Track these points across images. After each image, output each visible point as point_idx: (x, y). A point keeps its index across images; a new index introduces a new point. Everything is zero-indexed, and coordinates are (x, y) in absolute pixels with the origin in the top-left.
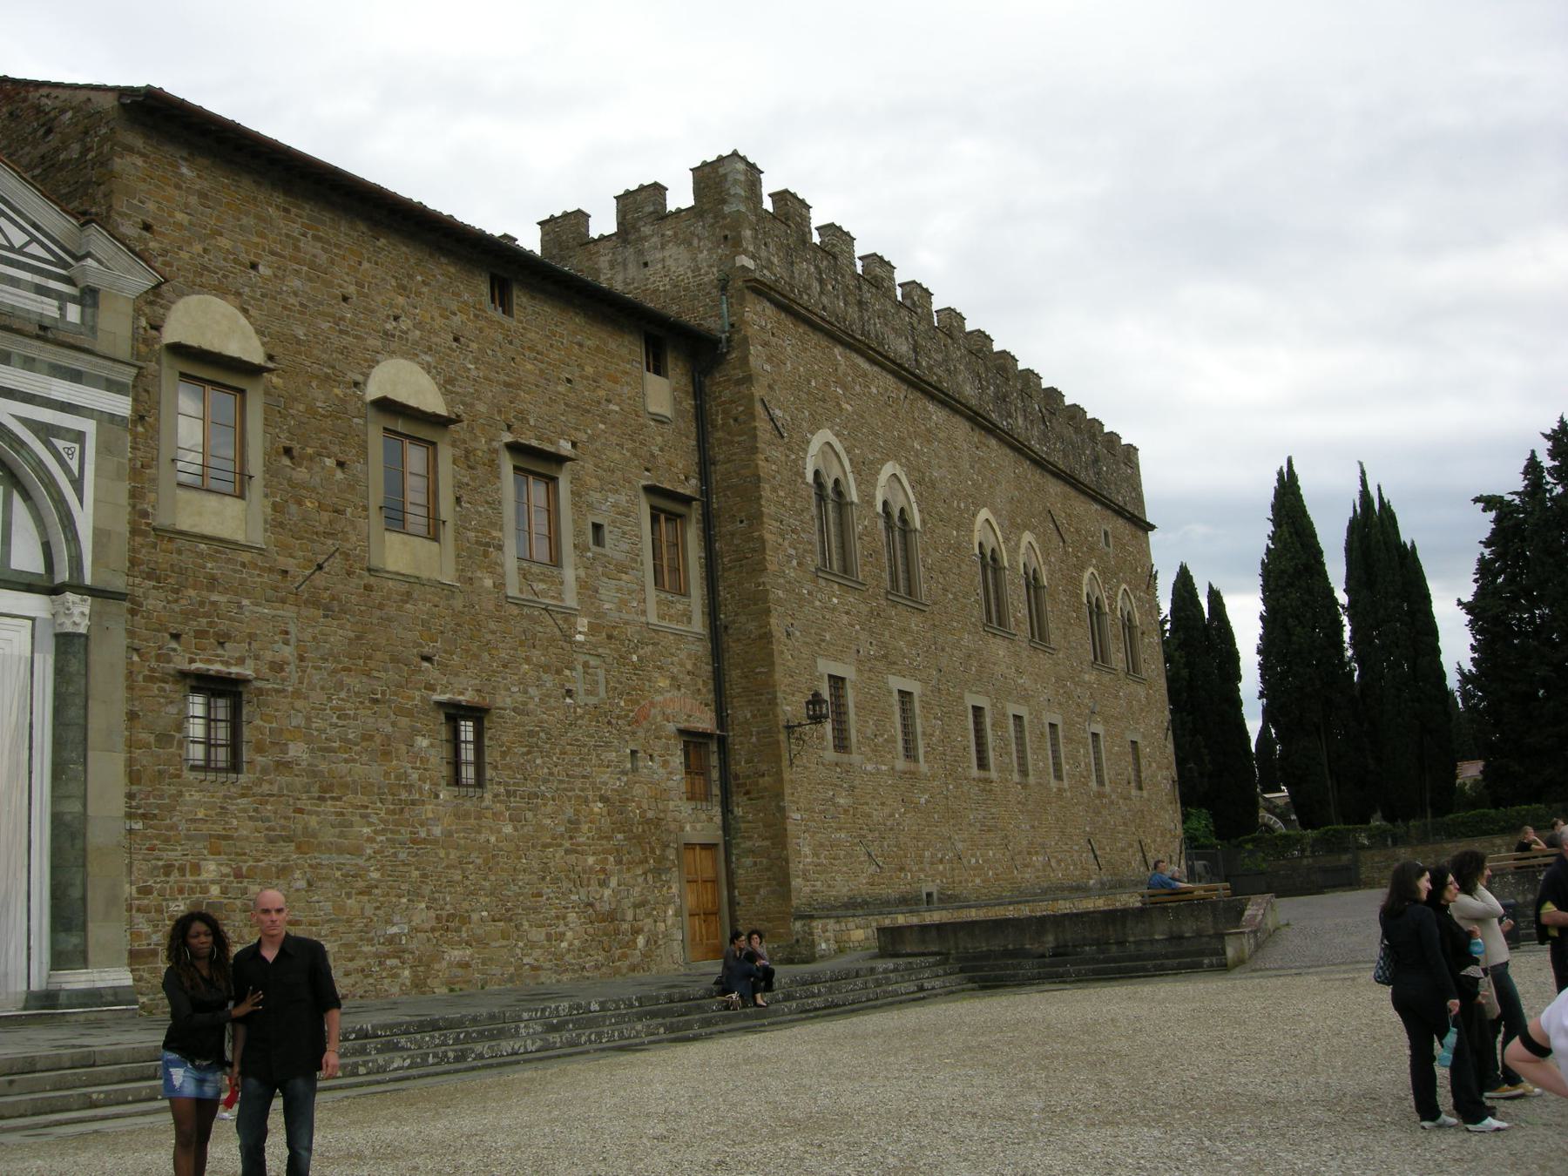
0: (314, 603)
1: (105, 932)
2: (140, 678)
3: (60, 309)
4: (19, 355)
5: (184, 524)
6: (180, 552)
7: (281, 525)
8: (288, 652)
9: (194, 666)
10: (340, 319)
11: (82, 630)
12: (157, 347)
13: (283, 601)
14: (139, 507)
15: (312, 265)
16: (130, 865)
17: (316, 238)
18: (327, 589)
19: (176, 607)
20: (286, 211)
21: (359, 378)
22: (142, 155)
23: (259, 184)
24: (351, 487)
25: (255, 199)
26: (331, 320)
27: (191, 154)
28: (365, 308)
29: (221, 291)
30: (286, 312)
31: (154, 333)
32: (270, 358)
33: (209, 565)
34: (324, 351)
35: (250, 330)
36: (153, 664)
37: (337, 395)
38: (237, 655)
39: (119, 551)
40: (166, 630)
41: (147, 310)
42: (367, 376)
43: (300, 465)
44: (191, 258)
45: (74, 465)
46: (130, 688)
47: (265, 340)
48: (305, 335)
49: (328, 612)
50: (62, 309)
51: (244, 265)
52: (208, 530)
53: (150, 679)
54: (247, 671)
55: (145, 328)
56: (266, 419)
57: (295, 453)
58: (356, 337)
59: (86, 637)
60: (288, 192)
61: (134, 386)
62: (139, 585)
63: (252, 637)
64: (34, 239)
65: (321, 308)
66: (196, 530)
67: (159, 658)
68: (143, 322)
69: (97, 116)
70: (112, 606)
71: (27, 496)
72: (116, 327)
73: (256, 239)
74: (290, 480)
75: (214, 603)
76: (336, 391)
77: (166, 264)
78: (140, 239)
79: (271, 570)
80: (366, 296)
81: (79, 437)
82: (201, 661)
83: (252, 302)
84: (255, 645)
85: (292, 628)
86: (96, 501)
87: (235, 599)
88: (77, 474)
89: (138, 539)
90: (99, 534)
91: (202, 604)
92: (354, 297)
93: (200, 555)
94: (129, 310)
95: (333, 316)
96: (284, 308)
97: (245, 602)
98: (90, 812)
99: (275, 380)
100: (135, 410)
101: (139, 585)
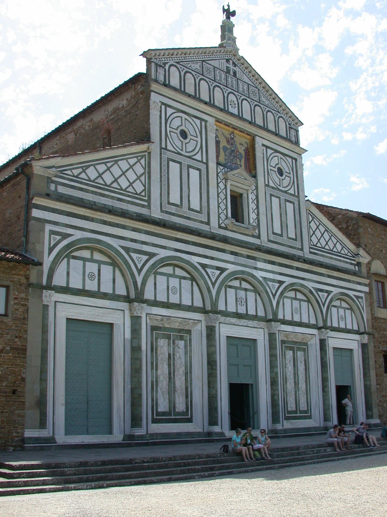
1: (375, 411)
9: (384, 349)
11: (367, 343)
16: (378, 396)
20: (385, 235)
22: (363, 228)
45: (362, 304)
46: (375, 355)
50: (355, 268)
53: (377, 353)
69: (351, 218)
71: (354, 313)
72: (364, 270)
81: (362, 298)
86: (366, 312)
89: (373, 321)
90: (367, 320)
98: (372, 384)
100: (369, 290)
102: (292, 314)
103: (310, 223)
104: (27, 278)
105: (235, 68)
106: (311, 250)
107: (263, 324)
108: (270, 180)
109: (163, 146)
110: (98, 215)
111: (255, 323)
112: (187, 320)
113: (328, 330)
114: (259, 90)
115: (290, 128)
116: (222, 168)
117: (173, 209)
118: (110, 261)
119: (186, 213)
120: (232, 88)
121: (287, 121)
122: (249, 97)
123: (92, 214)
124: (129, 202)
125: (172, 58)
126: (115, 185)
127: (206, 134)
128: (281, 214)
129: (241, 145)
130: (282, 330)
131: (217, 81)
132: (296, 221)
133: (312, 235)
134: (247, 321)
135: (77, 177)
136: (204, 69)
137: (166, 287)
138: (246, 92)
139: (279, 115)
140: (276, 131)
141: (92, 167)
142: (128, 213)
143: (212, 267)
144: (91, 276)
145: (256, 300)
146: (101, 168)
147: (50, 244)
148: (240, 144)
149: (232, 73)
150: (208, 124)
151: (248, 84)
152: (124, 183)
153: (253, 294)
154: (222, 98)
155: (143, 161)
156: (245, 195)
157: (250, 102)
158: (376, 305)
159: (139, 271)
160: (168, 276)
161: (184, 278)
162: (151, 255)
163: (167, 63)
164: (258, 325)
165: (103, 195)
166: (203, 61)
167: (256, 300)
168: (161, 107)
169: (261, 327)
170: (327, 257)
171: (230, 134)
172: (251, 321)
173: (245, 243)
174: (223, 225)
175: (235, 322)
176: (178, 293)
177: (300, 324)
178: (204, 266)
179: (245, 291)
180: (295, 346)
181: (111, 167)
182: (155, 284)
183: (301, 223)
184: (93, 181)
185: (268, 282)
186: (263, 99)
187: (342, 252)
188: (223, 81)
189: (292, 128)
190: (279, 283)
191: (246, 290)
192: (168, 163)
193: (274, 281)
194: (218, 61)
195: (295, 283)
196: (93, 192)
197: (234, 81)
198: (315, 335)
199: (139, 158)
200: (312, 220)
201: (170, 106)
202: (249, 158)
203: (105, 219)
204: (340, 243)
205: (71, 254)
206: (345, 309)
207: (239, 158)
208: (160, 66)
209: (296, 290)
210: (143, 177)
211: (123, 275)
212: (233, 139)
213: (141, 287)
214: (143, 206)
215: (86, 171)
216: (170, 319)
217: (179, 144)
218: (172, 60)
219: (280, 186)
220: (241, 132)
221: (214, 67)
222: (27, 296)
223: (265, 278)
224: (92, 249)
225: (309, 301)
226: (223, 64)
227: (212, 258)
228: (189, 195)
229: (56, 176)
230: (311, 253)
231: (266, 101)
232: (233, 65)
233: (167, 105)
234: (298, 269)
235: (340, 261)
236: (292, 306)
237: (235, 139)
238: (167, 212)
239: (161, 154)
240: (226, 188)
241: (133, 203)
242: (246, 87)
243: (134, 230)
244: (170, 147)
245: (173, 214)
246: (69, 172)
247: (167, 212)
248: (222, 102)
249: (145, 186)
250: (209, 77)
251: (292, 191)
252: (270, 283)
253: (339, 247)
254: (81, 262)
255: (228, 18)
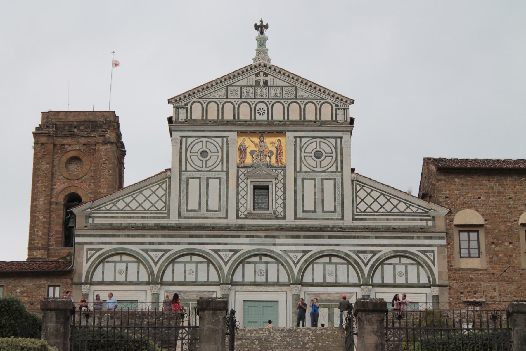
0: (504, 281)
2: (453, 304)
3: (427, 223)
4: (416, 237)
5: (463, 266)
6: (462, 273)
7: (492, 262)
8: (496, 294)
9: (467, 300)
10: (509, 205)
11: (437, 294)
12: (452, 226)
13: (494, 281)
14: (450, 265)
15: (499, 192)
17: (499, 185)
18: (507, 276)
19: (461, 286)
20: (489, 180)
21: (516, 219)
22: (445, 180)
23: (479, 176)
24: (515, 249)
25: (479, 180)
26: (506, 205)
27: (458, 175)
28: (518, 199)
29: (470, 207)
30: (490, 208)
31: (451, 223)
32: (486, 220)
33: (470, 275)
34: (504, 214)
35: (480, 215)
36: (456, 300)
37: (508, 226)
38: (480, 296)
39: (445, 276)
40: (459, 292)
41: (449, 218)
42: (519, 218)
43: (497, 246)
44: (460, 202)
45: (432, 258)
47: (484, 216)
48: (497, 212)
49: (508, 282)
51: (476, 199)
52: (469, 267)
54: (483, 300)
55: (448, 222)
56: (485, 236)
57: (495, 243)
58: (514, 208)
59: (437, 296)
60: (489, 175)
61: (446, 237)
62: (451, 283)
63: (484, 291)
64: (419, 209)
65: (502, 203)
66: (466, 267)
67: (457, 299)
68: (448, 221)
70: (444, 288)
71: (422, 267)
72: (441, 224)
73: (479, 191)
74: (494, 250)
75: (472, 284)
76: (508, 224)
77: (453, 205)
78: (445, 201)
79: (489, 274)
80: (518, 195)
81: (433, 252)
82: (470, 298)
83: (480, 208)
84: (485, 293)
85: (497, 288)
86: (438, 265)
87: (479, 282)
88: (433, 260)
90: (440, 273)
91: (469, 285)
92: (514, 197)
93: (468, 273)
94: (444, 219)
95: (506, 204)
96: (490, 206)
97: (482, 283)
99: (488, 226)
100: (447, 242)
101: (451, 283)
102: (324, 277)
103: (357, 193)
104: (72, 280)
105: (266, 78)
106: (356, 217)
107: (284, 288)
108: (303, 166)
109: (183, 169)
110: (122, 232)
111: (276, 288)
112: (201, 292)
113: (370, 287)
114: (296, 87)
115: (336, 109)
116: (243, 170)
117: (191, 214)
118: (136, 260)
119: (203, 214)
120: (262, 98)
121: (334, 103)
122: (283, 99)
123: (117, 232)
124: (151, 218)
125: (194, 96)
126: (140, 208)
127: (228, 147)
128: (315, 193)
129: (272, 144)
130: (309, 291)
131: (244, 98)
132: (337, 195)
133: (360, 203)
134: (266, 287)
135: (109, 210)
136: (229, 92)
137: (183, 271)
138: (279, 95)
139: (323, 101)
140: (316, 118)
141: (121, 201)
142: (147, 226)
143: (225, 251)
144: (121, 272)
145: (278, 270)
146: (128, 200)
147: (87, 257)
148: (271, 143)
149: (262, 84)
150: (229, 139)
151: (282, 87)
152: (147, 205)
153: (276, 265)
154: (249, 110)
155: (164, 186)
156: (270, 187)
157: (283, 102)
158: (456, 255)
159: (156, 263)
160: (185, 263)
161: (201, 262)
162: (166, 251)
163: (189, 102)
164: (280, 289)
165: (130, 218)
166: (228, 86)
167: (278, 270)
168: (181, 141)
169: (283, 290)
170: (380, 220)
171: (260, 139)
172: (272, 287)
173: (264, 226)
174: (243, 216)
175: (253, 289)
176: (195, 274)
177: (335, 285)
178: (216, 251)
179: (265, 264)
180: (331, 304)
181: (136, 197)
182: (173, 270)
183: (342, 195)
184: (122, 210)
185: (290, 254)
186: (301, 94)
187: (408, 210)
188: (251, 95)
189: (339, 109)
190: (303, 253)
191: (267, 263)
192: (188, 181)
193: (297, 252)
194: (246, 79)
195: (324, 250)
196: (121, 217)
197: (264, 91)
198: (356, 292)
199: (160, 184)
200: (362, 188)
201: (190, 137)
202: (282, 153)
203: (128, 233)
204: (404, 203)
205: (106, 260)
206: (406, 265)
207: (269, 156)
208: (181, 108)
209: (330, 256)
210: (165, 196)
211: (146, 267)
212: (261, 142)
213: (157, 273)
214: (163, 218)
215: (116, 205)
216: (186, 293)
217: (199, 163)
218: (195, 98)
219: (317, 168)
220: (270, 133)
221: (241, 86)
222: (72, 290)
223: (286, 251)
224: (121, 254)
225: (349, 263)
226: (251, 80)
227: (226, 244)
228: (207, 201)
229: (93, 213)
230: (356, 219)
231: (306, 94)
232: (264, 76)
233: (186, 137)
234: (330, 237)
235: (403, 220)
236: (324, 270)
237: (264, 141)
238: (185, 218)
239: (180, 176)
240: (247, 186)
241: (154, 218)
242: (279, 90)
243: (152, 236)
244: (189, 168)
245: (191, 218)
246: (103, 208)
247: (185, 218)
248: (249, 114)
249: (165, 203)
250: (234, 97)
251: (333, 169)
252: (291, 255)
253: (402, 207)
254: (113, 264)
255: (262, 33)
